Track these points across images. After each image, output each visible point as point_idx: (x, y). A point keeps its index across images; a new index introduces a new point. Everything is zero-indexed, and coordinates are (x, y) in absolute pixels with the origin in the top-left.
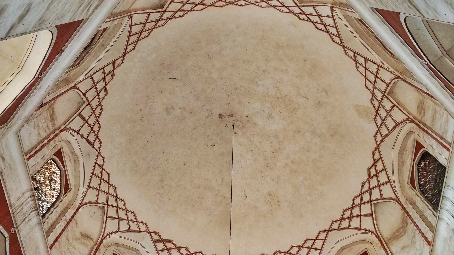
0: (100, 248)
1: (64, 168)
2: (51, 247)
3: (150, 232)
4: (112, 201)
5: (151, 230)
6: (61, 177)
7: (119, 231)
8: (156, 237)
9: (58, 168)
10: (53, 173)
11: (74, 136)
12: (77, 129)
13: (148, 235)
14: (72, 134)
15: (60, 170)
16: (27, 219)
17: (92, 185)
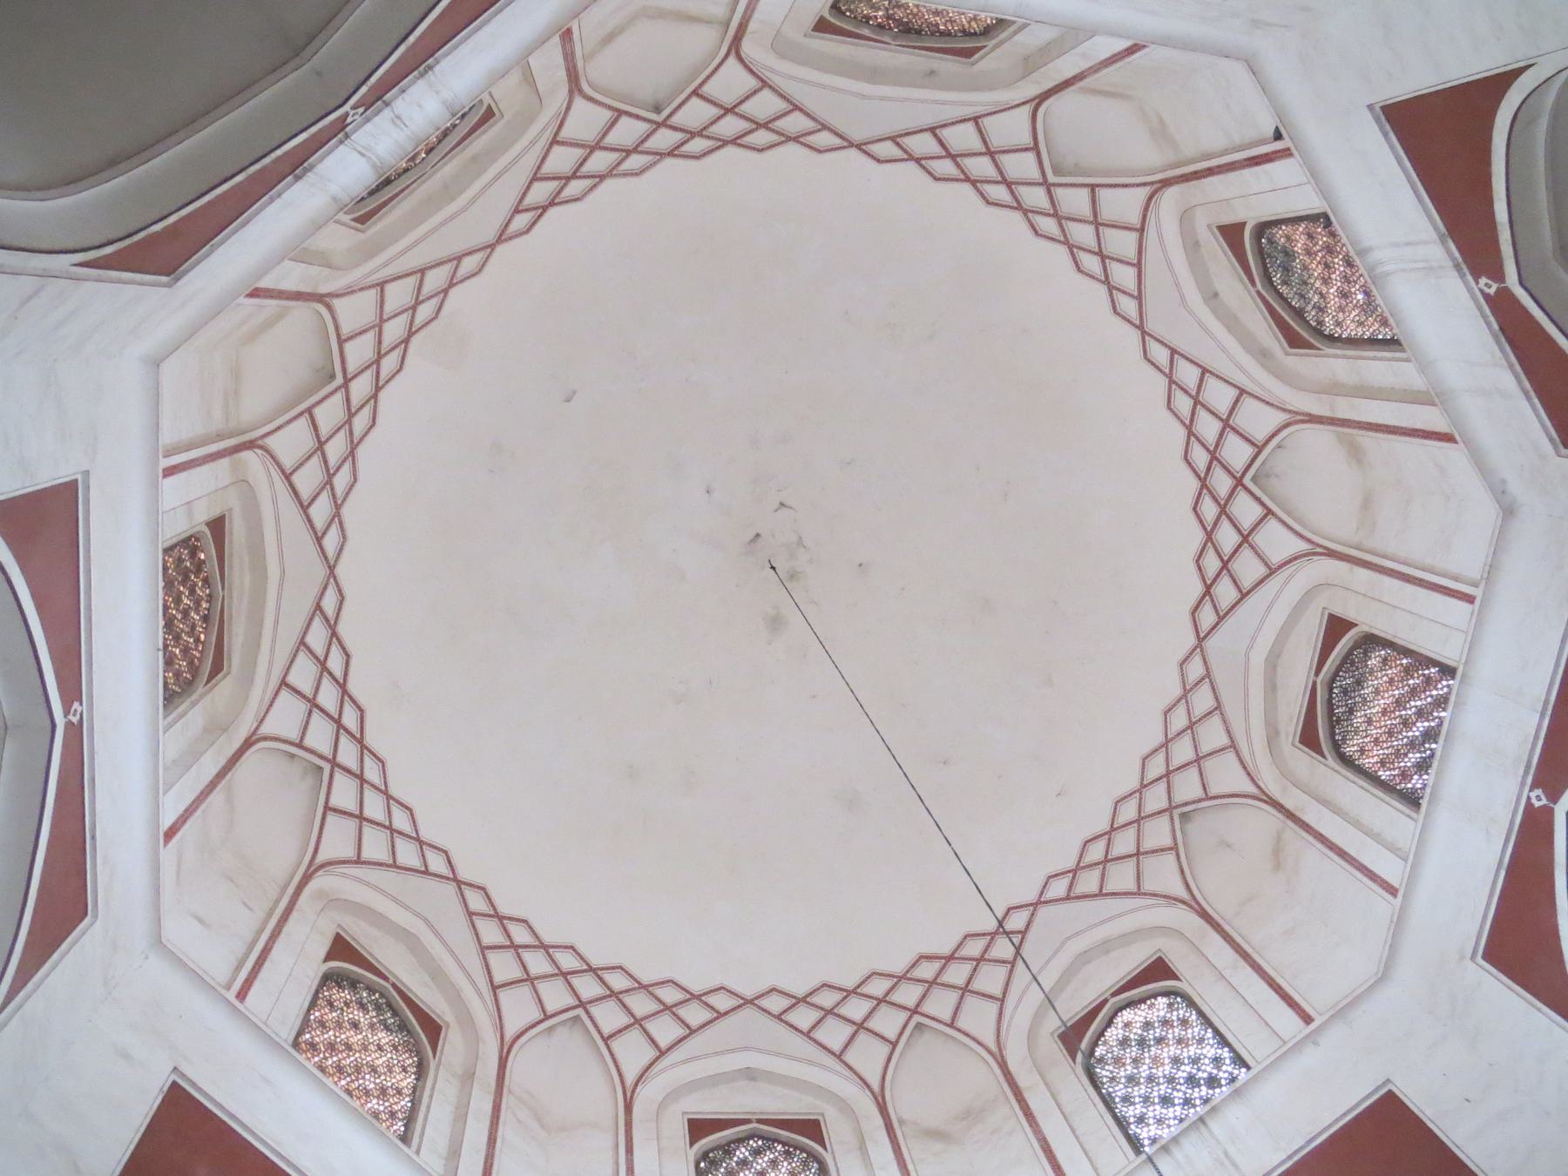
0: (1289, 805)
1: (1105, 1001)
2: (1307, 1019)
3: (1201, 640)
4: (1156, 799)
5: (1191, 640)
6: (1131, 1004)
7: (1233, 745)
8: (1207, 617)
9: (1110, 1023)
10: (1124, 1043)
11: (1016, 1007)
12: (993, 1008)
13: (1209, 644)
14: (1012, 1017)
15: (1115, 1014)
16: (1232, 1151)
17: (1131, 885)
